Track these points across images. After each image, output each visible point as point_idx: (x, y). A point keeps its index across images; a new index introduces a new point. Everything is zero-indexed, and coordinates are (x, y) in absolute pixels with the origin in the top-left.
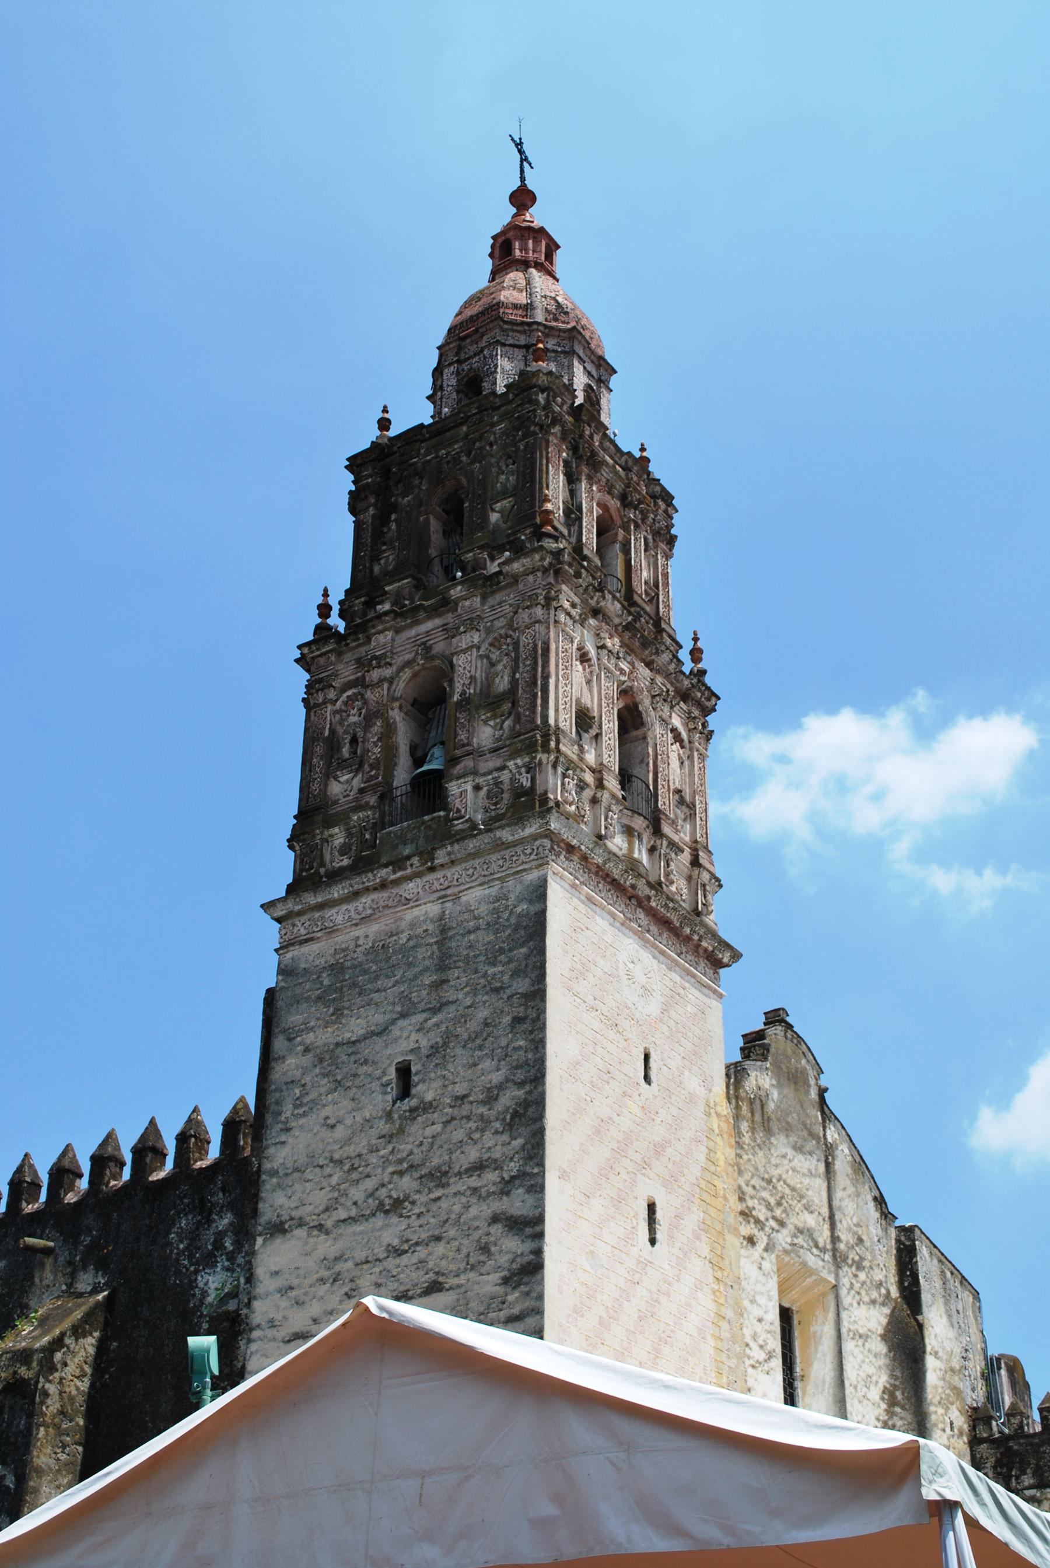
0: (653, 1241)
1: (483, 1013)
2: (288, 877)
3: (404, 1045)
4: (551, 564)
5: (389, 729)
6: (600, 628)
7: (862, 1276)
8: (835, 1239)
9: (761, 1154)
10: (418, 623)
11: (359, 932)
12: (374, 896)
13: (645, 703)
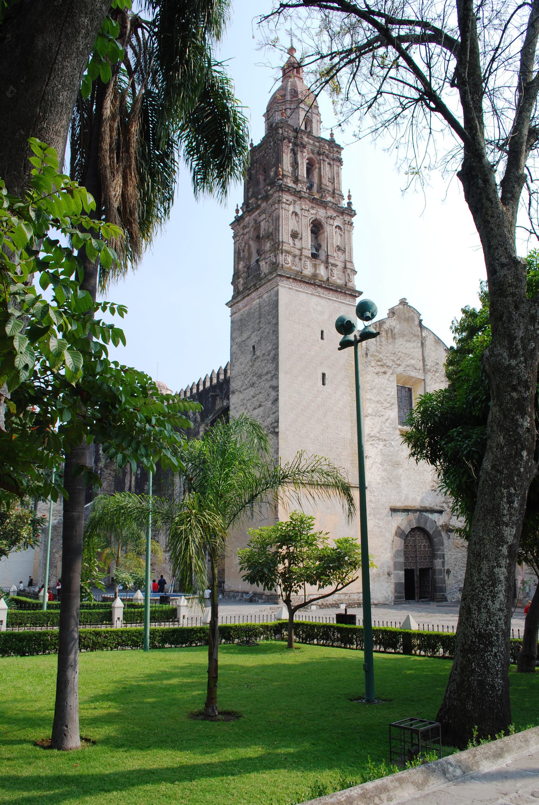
0: (324, 384)
1: (267, 330)
2: (232, 294)
3: (254, 341)
5: (249, 247)
6: (301, 204)
7: (437, 374)
8: (424, 365)
9: (390, 346)
10: (254, 213)
11: (244, 309)
12: (247, 298)
13: (323, 221)
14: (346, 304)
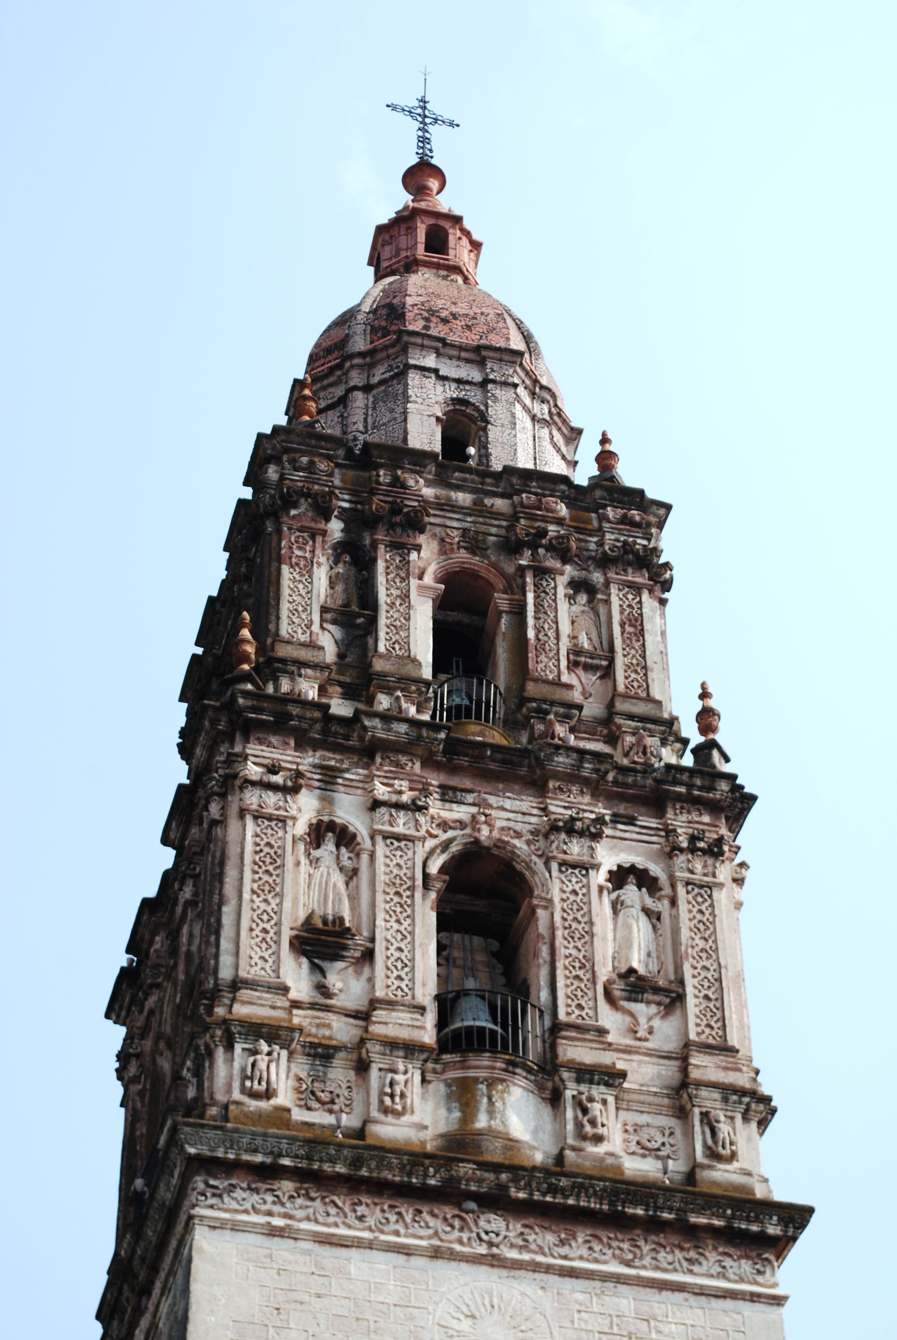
4: (231, 722)
14: (701, 1292)
